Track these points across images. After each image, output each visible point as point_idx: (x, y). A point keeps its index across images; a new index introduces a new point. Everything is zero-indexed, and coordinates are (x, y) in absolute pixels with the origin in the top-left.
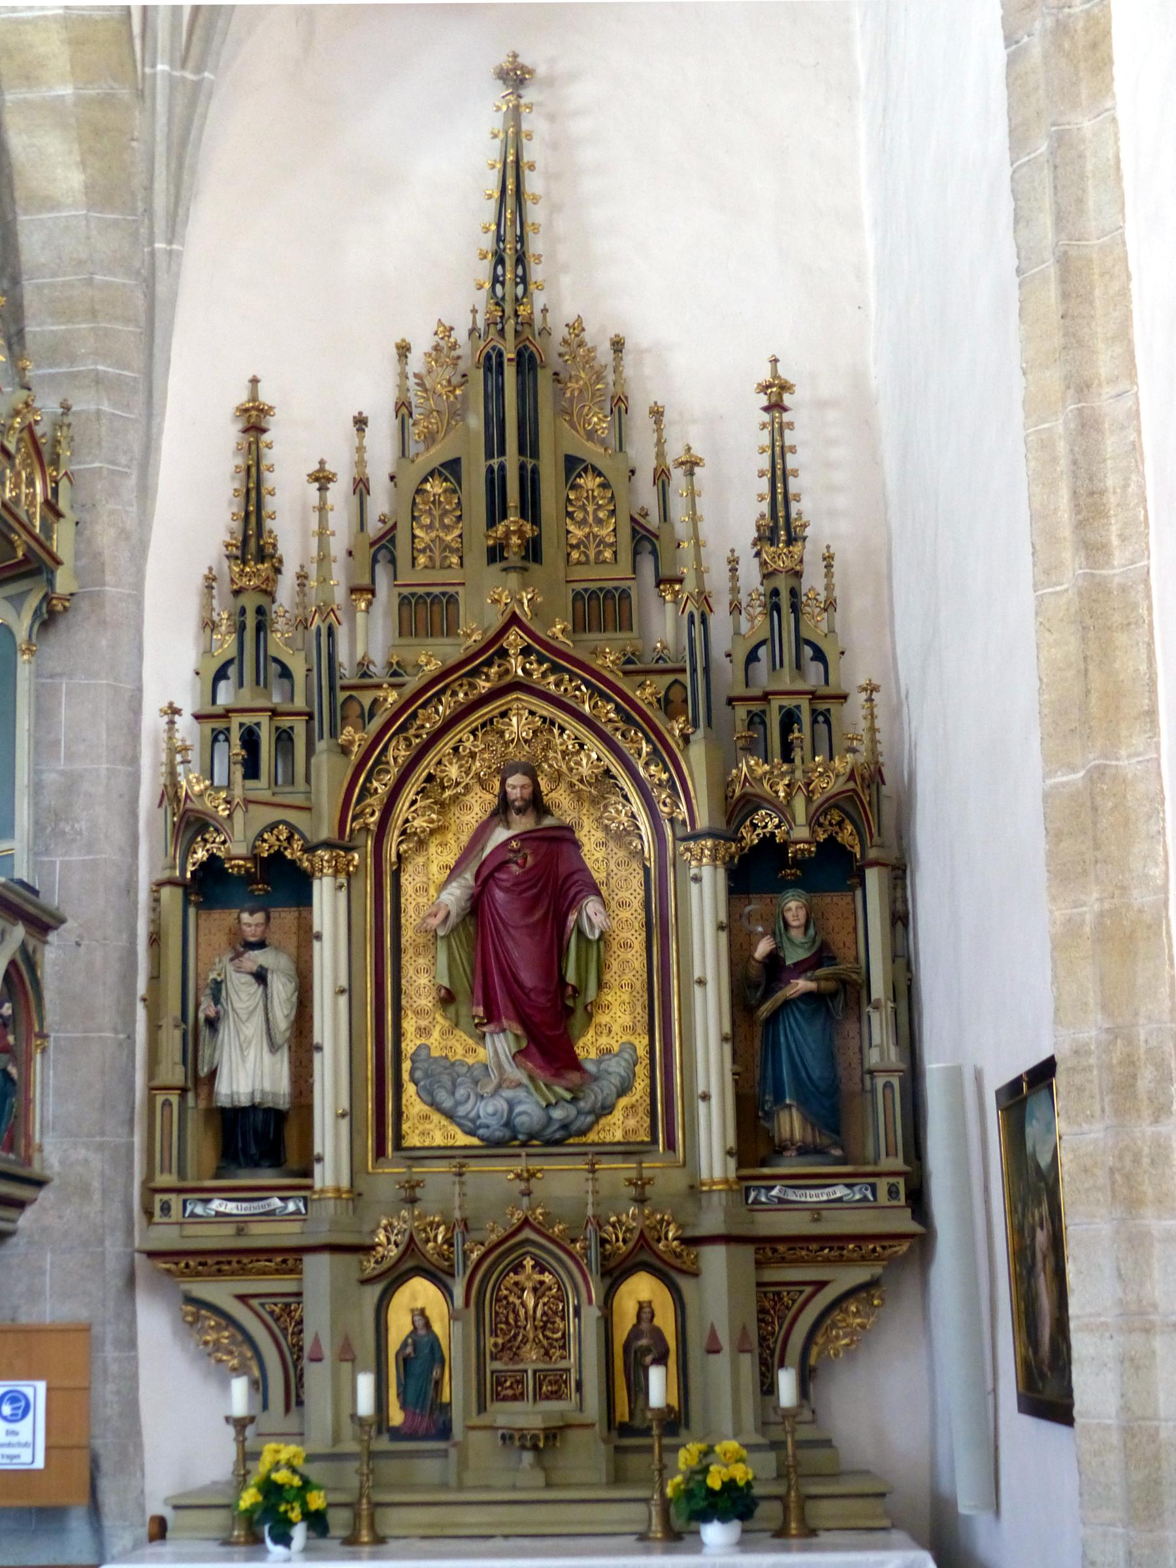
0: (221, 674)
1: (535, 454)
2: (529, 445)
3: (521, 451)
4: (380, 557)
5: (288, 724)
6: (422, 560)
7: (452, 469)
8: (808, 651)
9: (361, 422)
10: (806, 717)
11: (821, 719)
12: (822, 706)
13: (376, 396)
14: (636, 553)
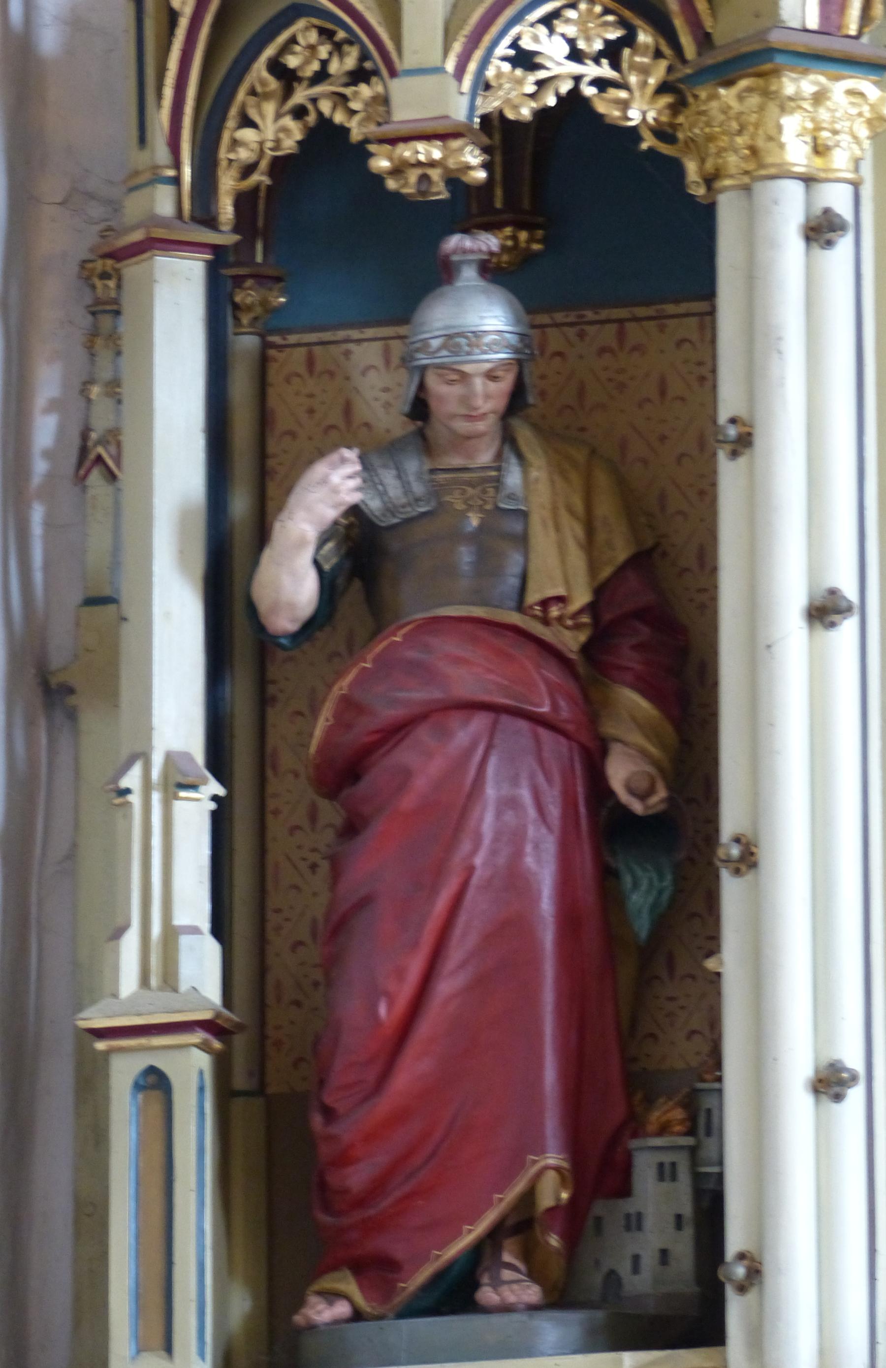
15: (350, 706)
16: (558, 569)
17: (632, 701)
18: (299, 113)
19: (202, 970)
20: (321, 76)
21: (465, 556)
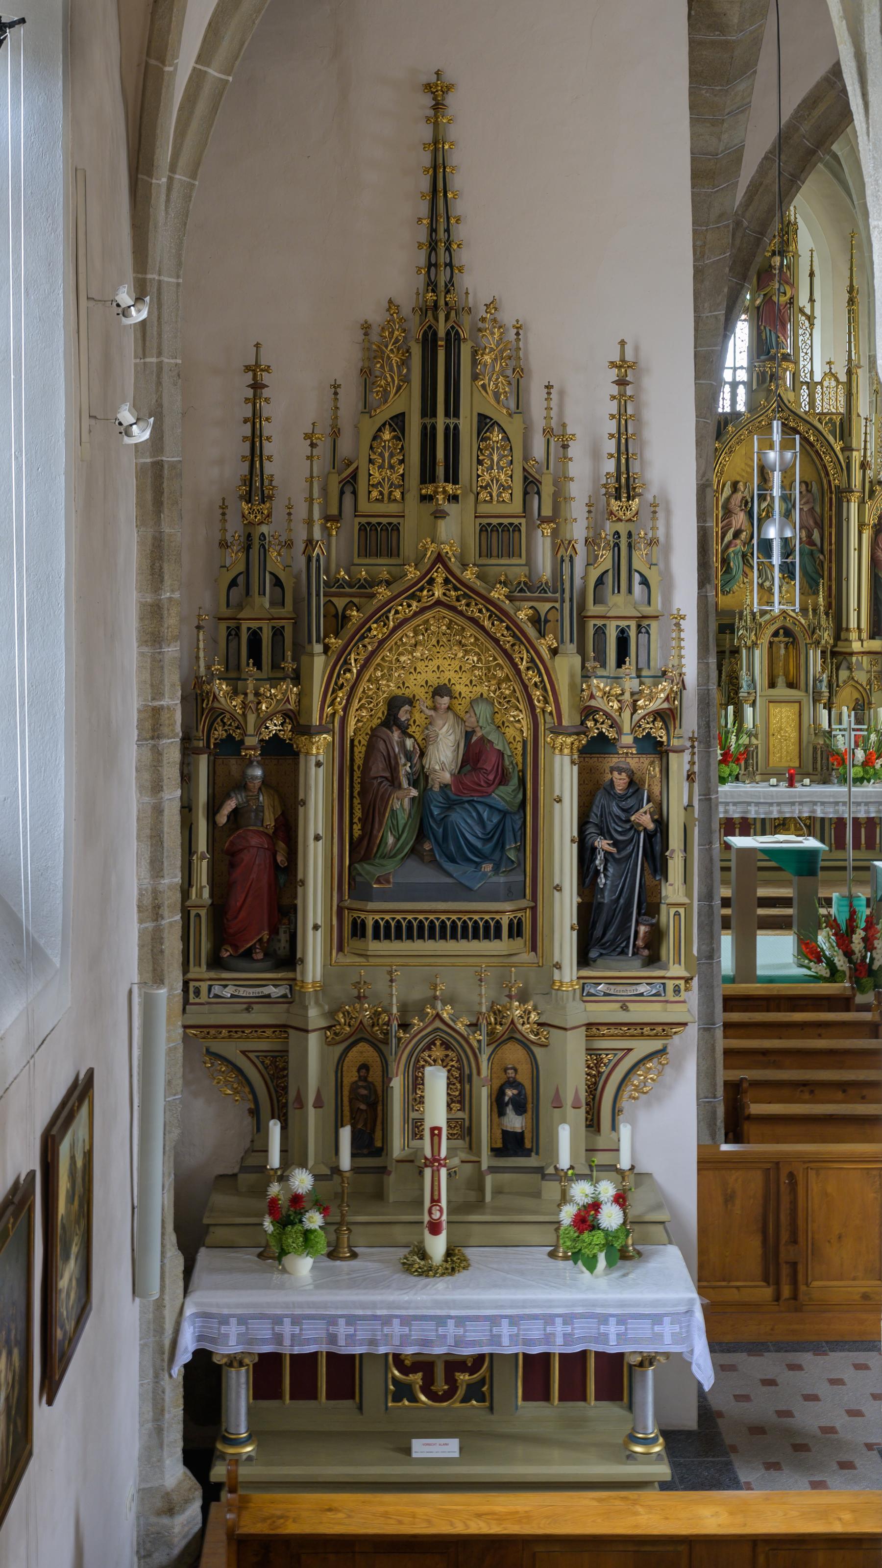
0: (233, 583)
1: (457, 415)
2: (453, 410)
3: (447, 414)
4: (345, 489)
5: (281, 625)
6: (375, 494)
7: (398, 422)
8: (637, 578)
9: (336, 387)
10: (633, 633)
11: (643, 630)
12: (645, 623)
13: (342, 360)
14: (526, 493)
15: (232, 843)
16: (269, 820)
17: (281, 845)
18: (226, 731)
19: (206, 893)
20: (230, 725)
21: (253, 814)
